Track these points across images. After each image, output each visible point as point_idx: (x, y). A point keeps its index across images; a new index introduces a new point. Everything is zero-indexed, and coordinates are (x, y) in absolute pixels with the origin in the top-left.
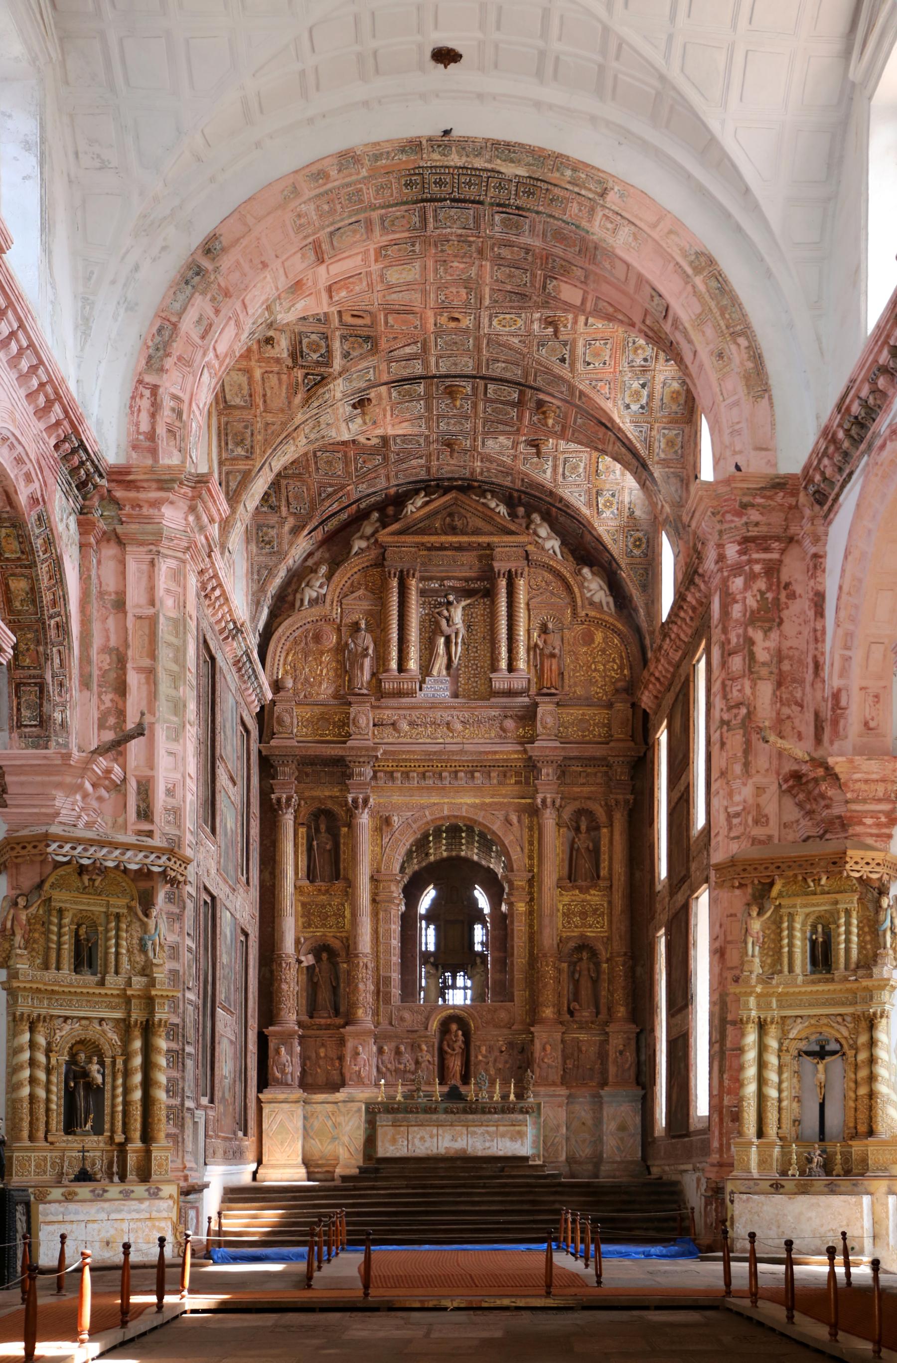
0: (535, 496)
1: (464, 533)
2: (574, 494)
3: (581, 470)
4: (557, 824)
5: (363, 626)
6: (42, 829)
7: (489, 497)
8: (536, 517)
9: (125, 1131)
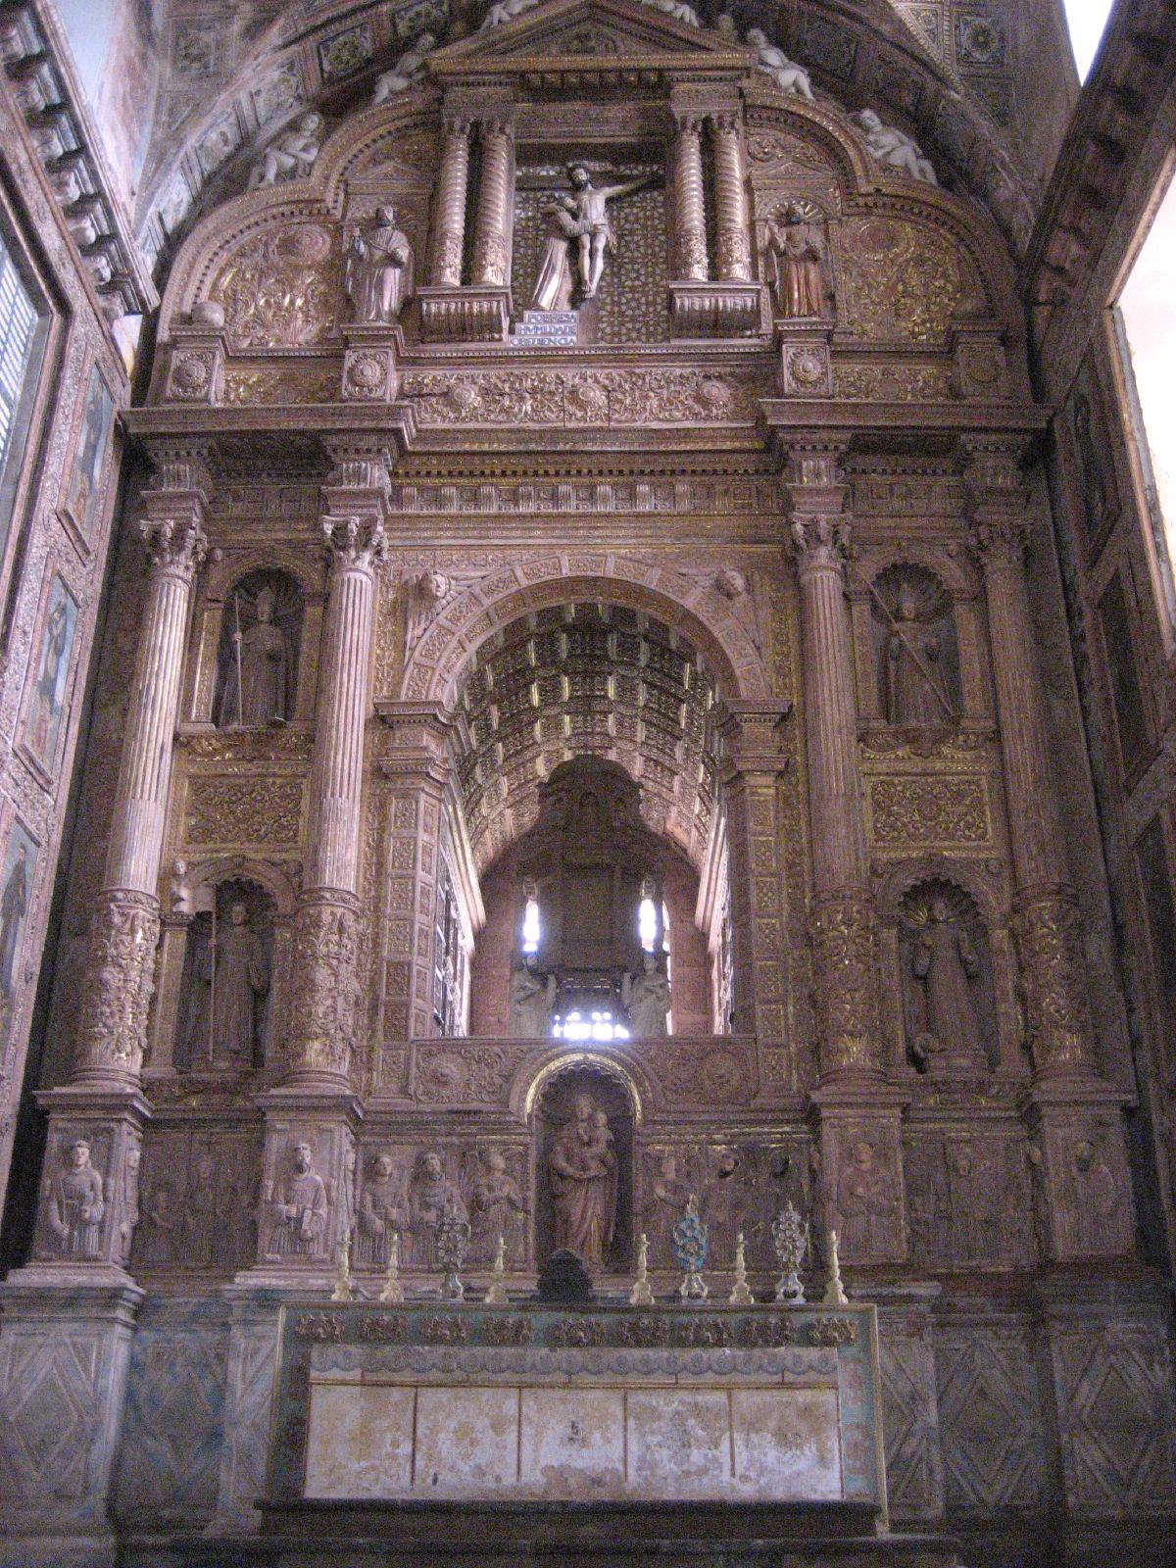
4: (846, 596)
5: (390, 216)
8: (756, 34)
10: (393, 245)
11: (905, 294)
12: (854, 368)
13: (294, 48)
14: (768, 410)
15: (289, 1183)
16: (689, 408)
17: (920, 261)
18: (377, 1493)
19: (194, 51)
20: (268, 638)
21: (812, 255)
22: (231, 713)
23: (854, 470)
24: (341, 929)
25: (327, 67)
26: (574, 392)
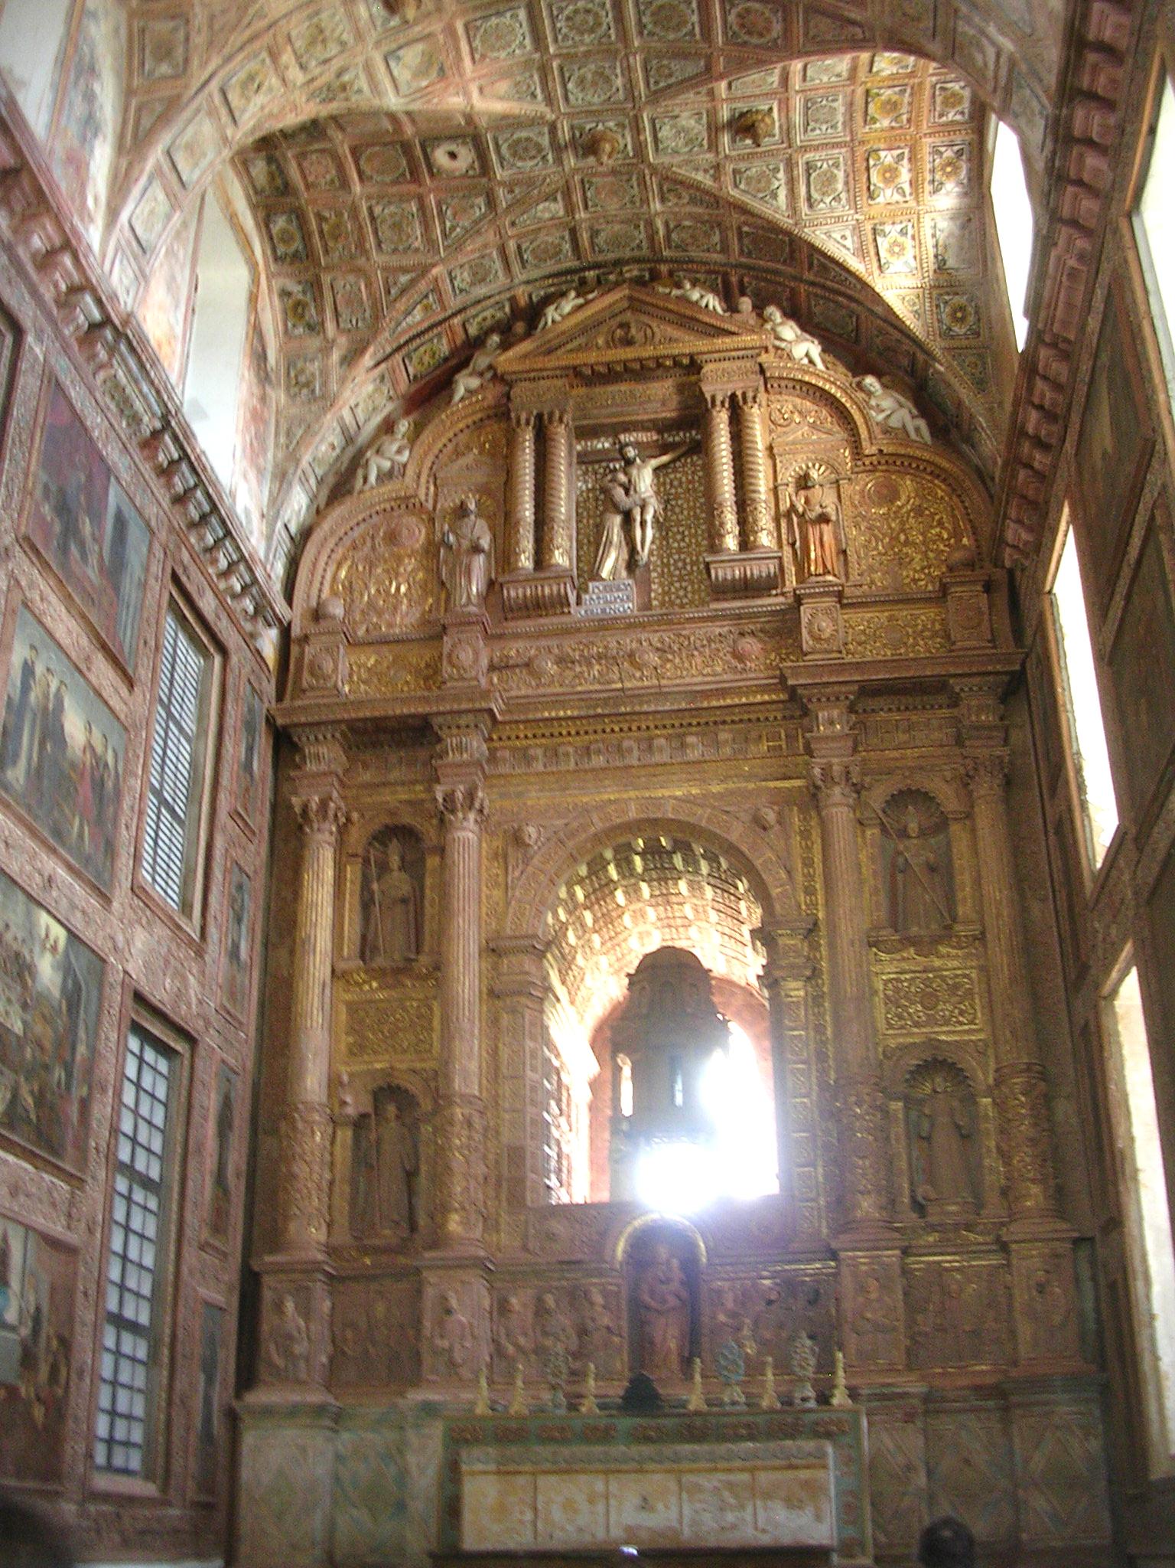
0: (767, 270)
1: (649, 339)
2: (836, 239)
3: (840, 186)
5: (472, 506)
7: (688, 286)
8: (774, 313)
10: (477, 532)
11: (906, 543)
12: (861, 619)
13: (383, 366)
14: (788, 673)
15: (441, 1324)
16: (728, 662)
17: (918, 511)
18: (511, 1545)
19: (302, 379)
20: (399, 882)
21: (824, 519)
22: (375, 949)
23: (865, 711)
24: (469, 1124)
25: (411, 370)
26: (631, 655)
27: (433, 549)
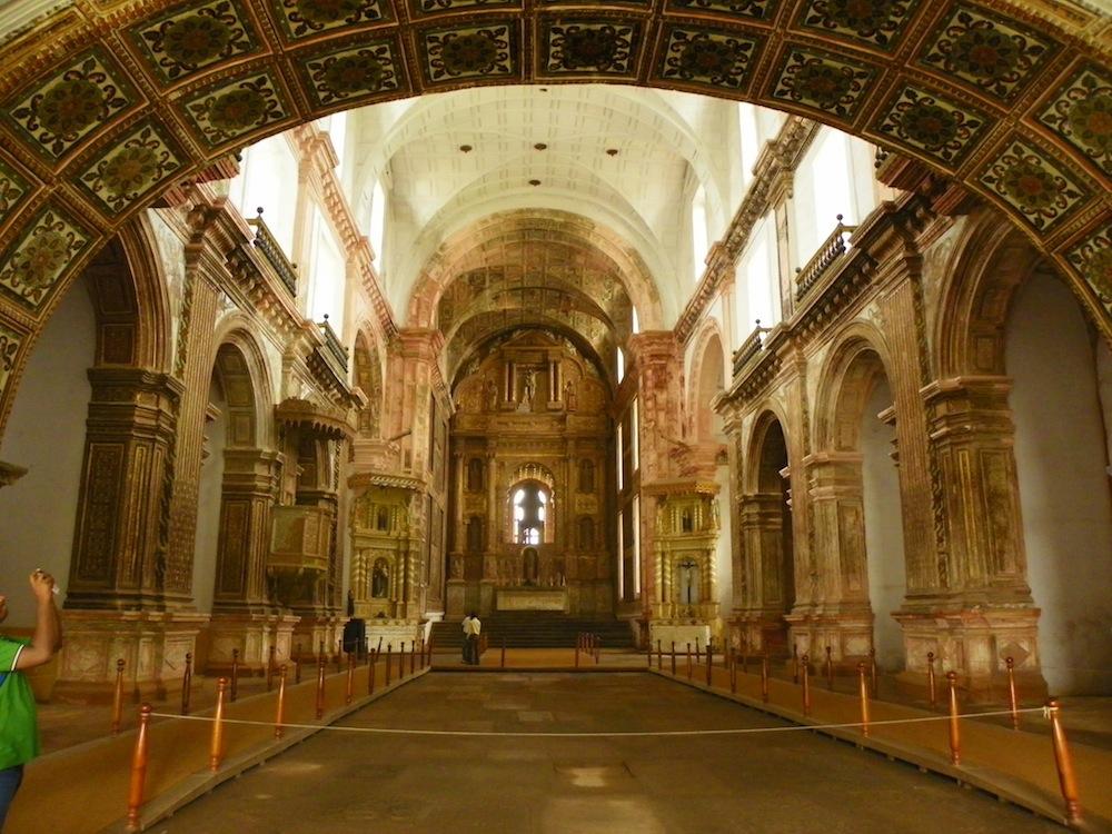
1: (536, 345)
2: (583, 333)
6: (368, 472)
9: (396, 596)
27: (484, 392)
